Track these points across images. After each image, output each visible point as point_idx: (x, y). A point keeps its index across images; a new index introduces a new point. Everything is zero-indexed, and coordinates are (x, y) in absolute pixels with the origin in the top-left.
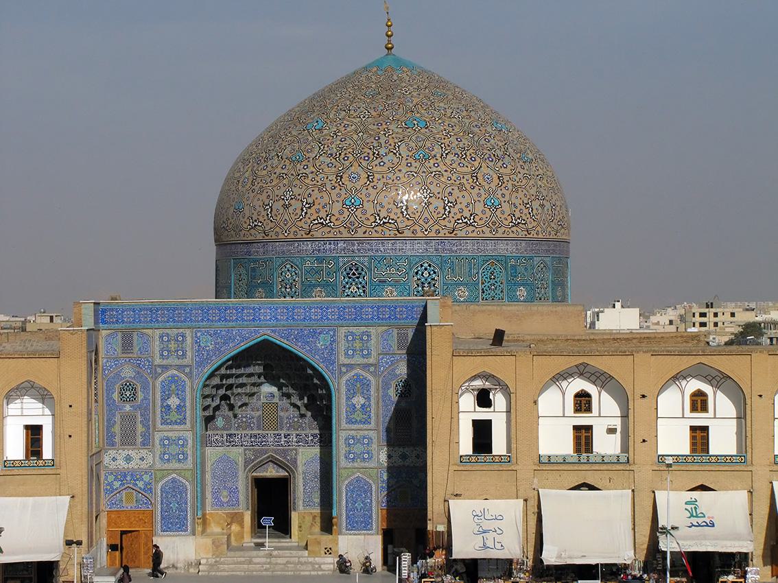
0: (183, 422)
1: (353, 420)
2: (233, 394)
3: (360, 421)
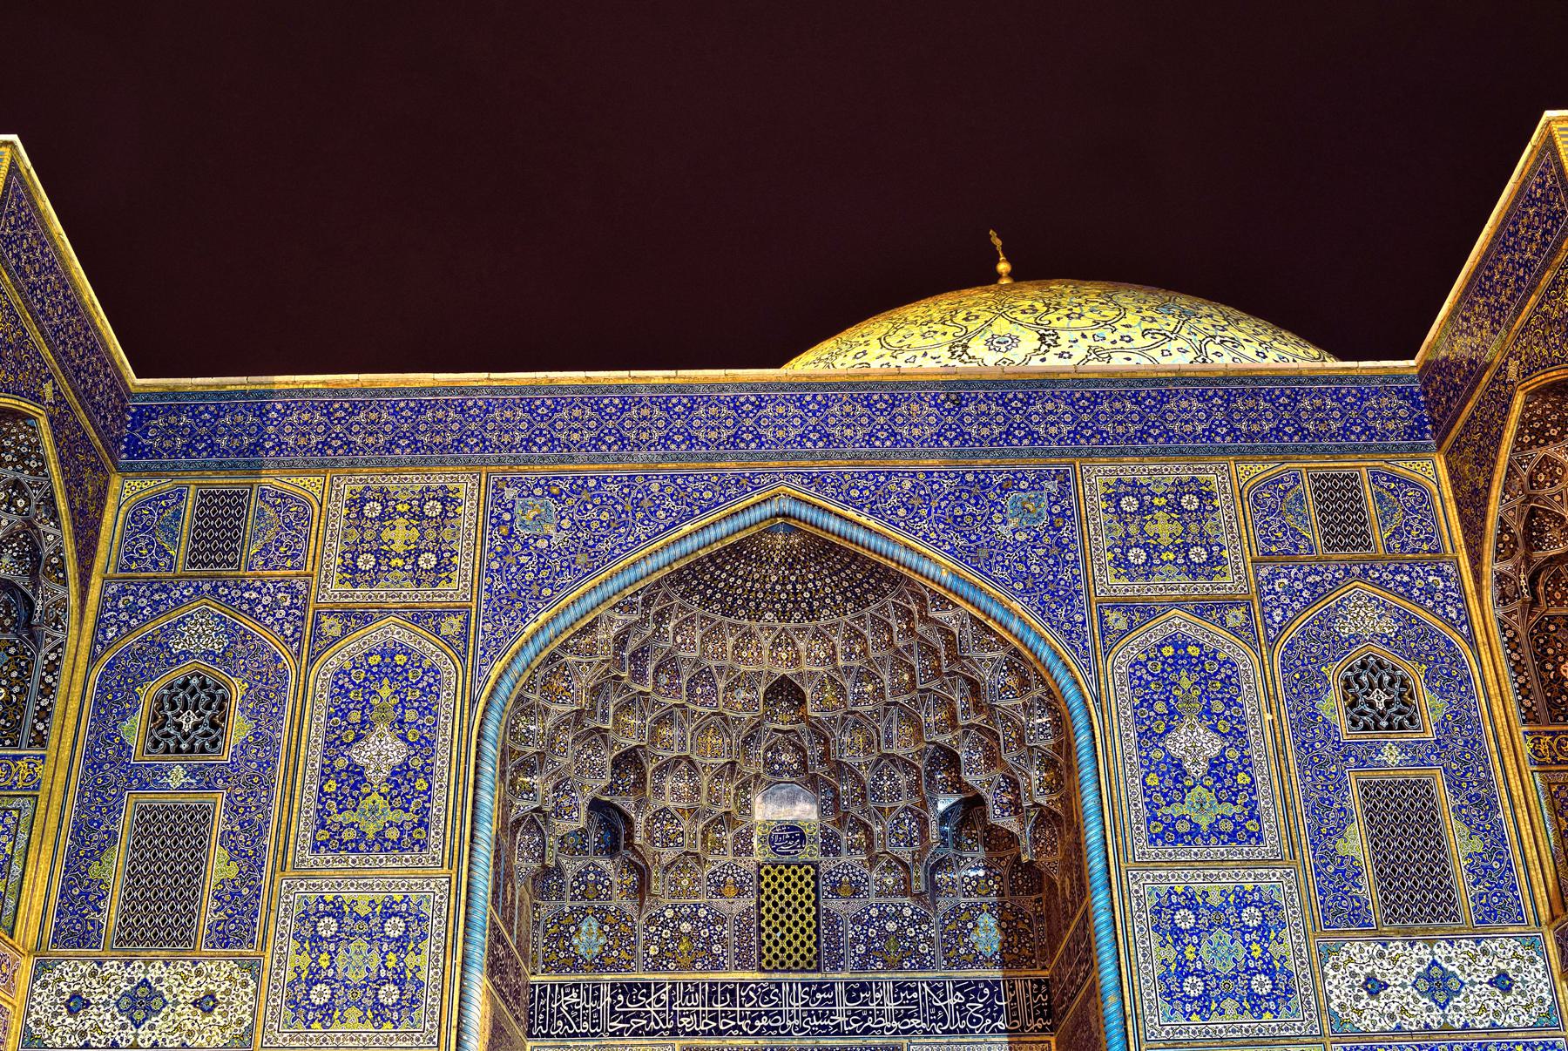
0: (411, 839)
1: (1183, 827)
3: (1214, 830)
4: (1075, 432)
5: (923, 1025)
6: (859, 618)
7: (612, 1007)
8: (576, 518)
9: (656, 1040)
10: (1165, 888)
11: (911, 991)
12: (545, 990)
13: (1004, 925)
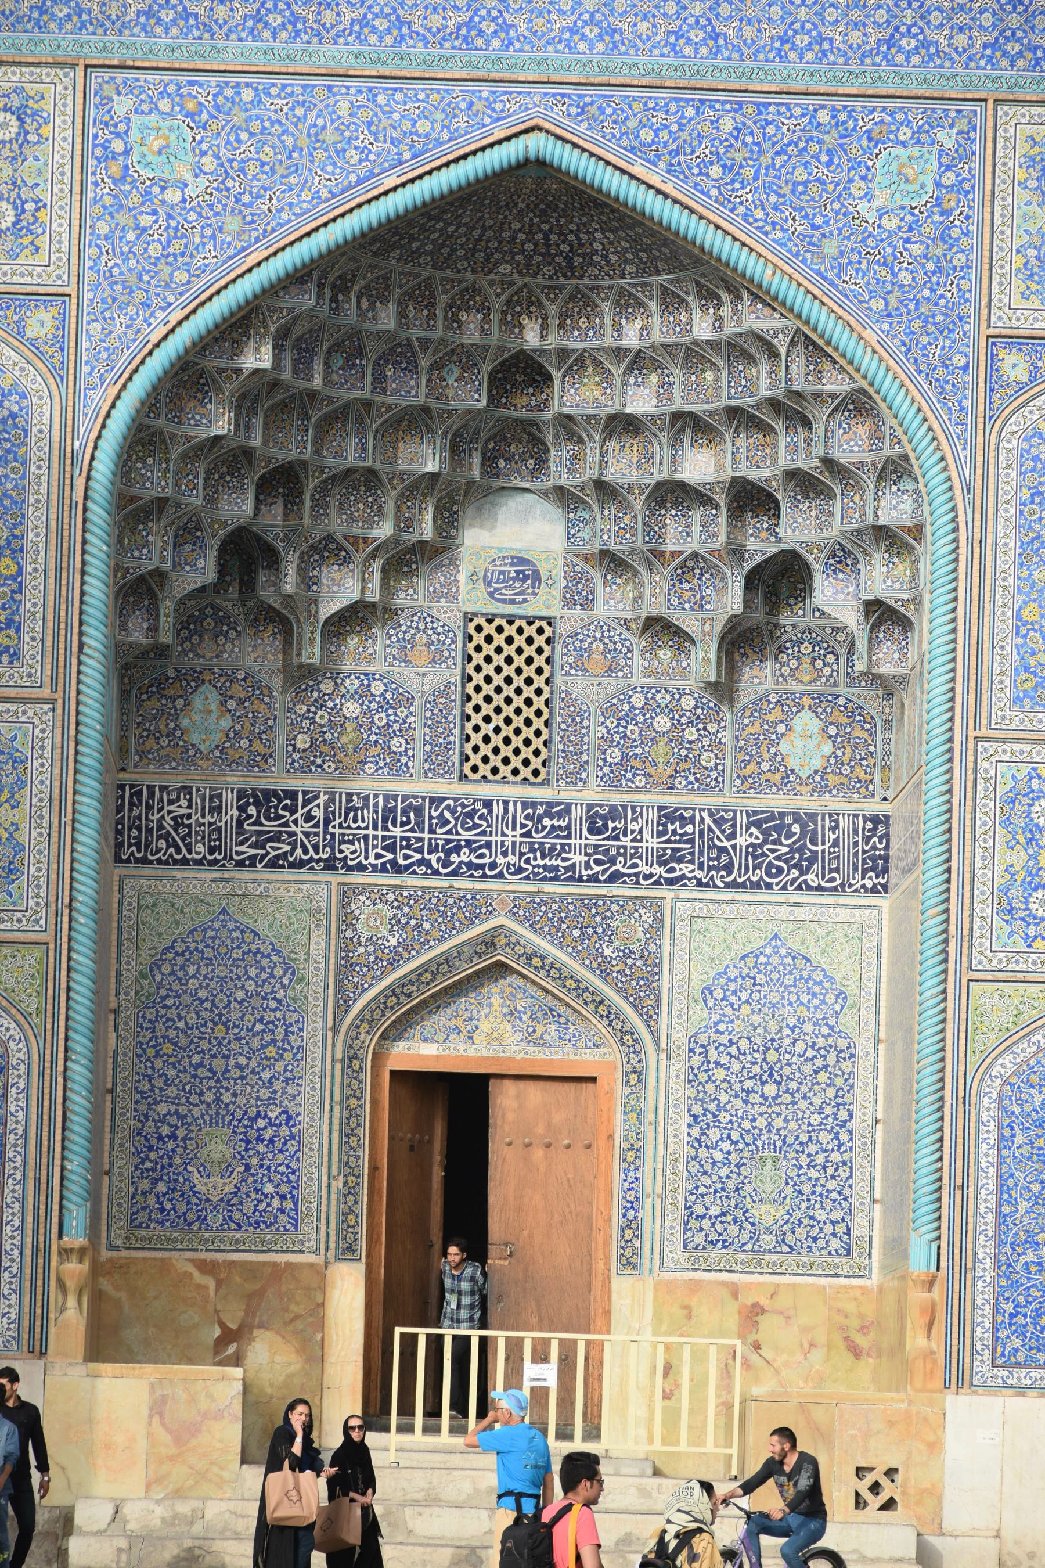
2: (290, 534)
4: (994, 45)
5: (699, 874)
6: (642, 285)
7: (240, 823)
8: (225, 154)
9: (303, 874)
10: (1026, 768)
11: (684, 821)
12: (139, 793)
13: (832, 730)
